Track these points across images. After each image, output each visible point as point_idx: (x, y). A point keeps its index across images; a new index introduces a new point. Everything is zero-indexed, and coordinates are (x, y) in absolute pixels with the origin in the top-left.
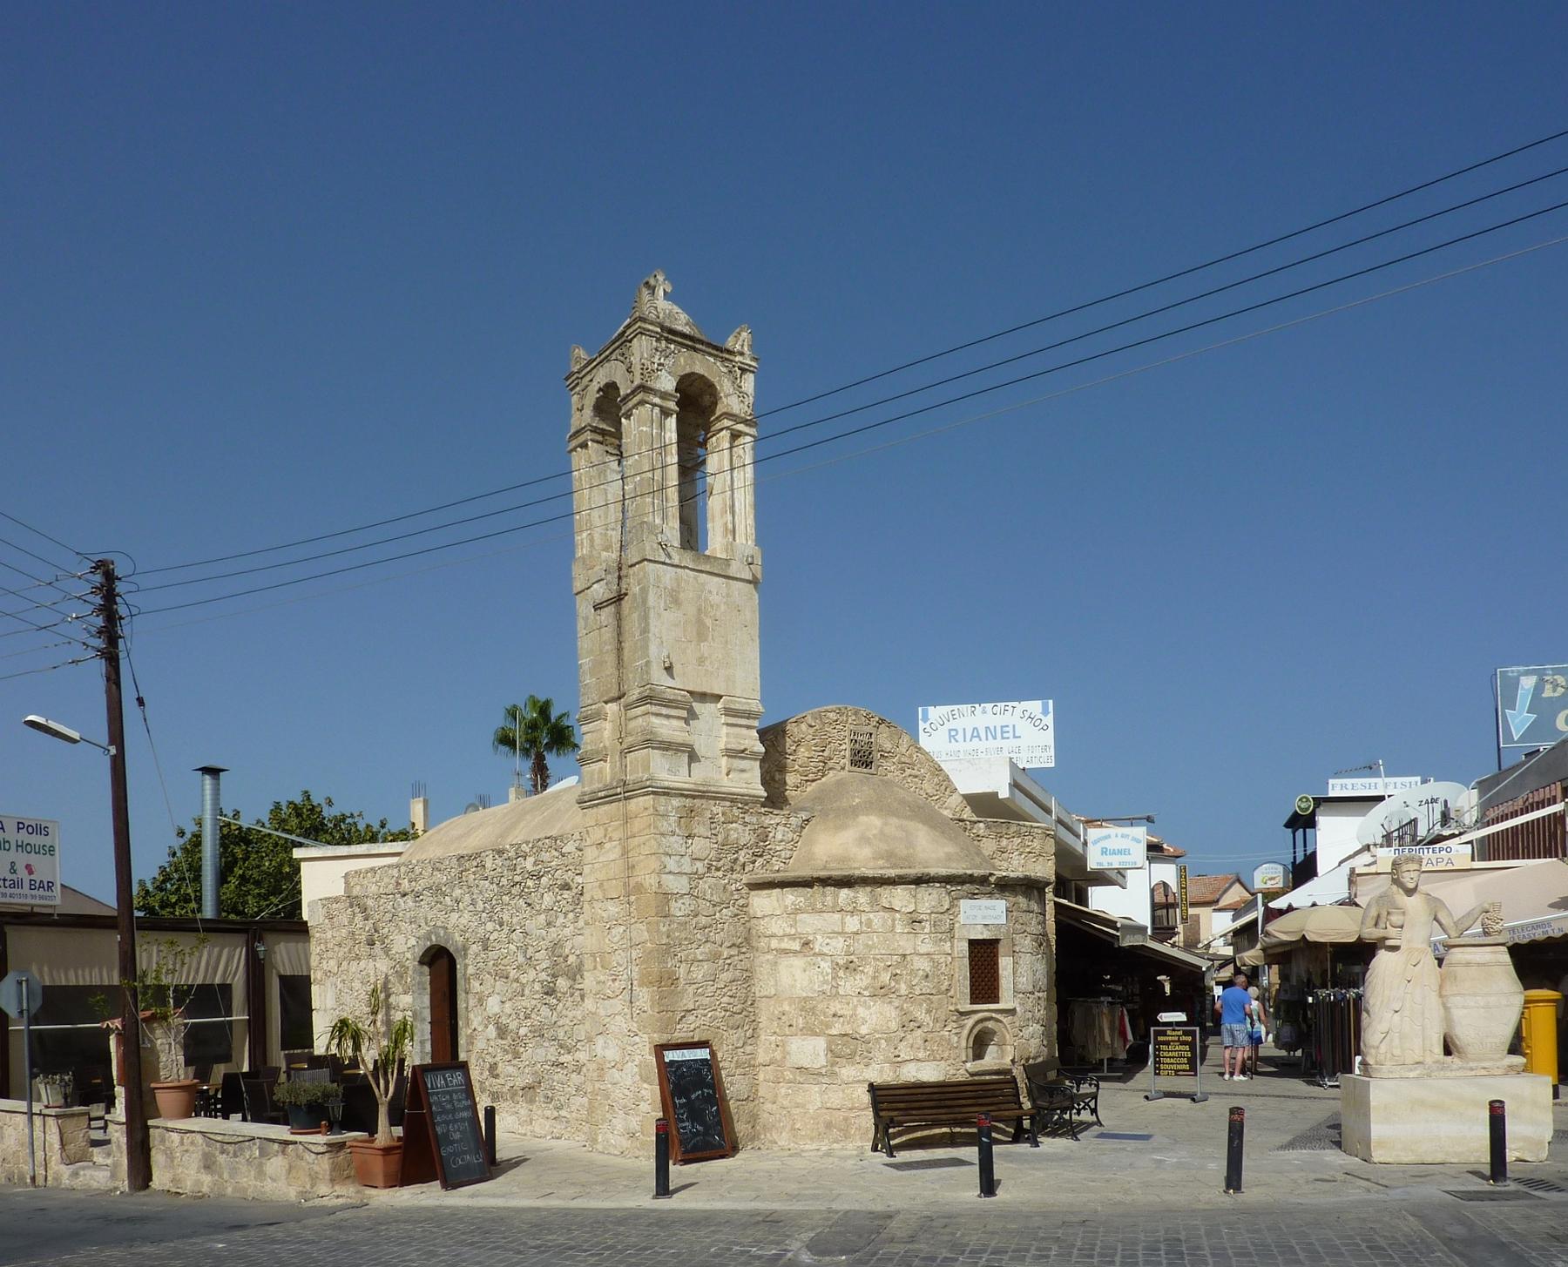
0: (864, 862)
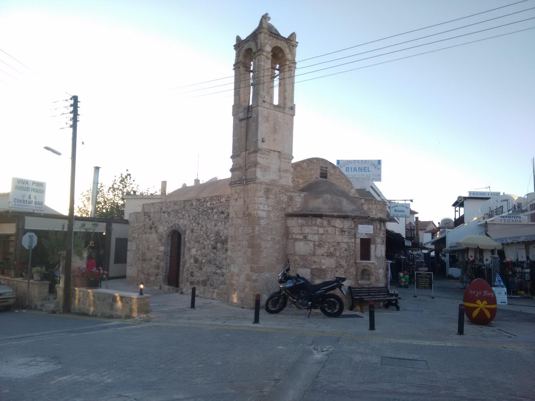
0: (325, 209)
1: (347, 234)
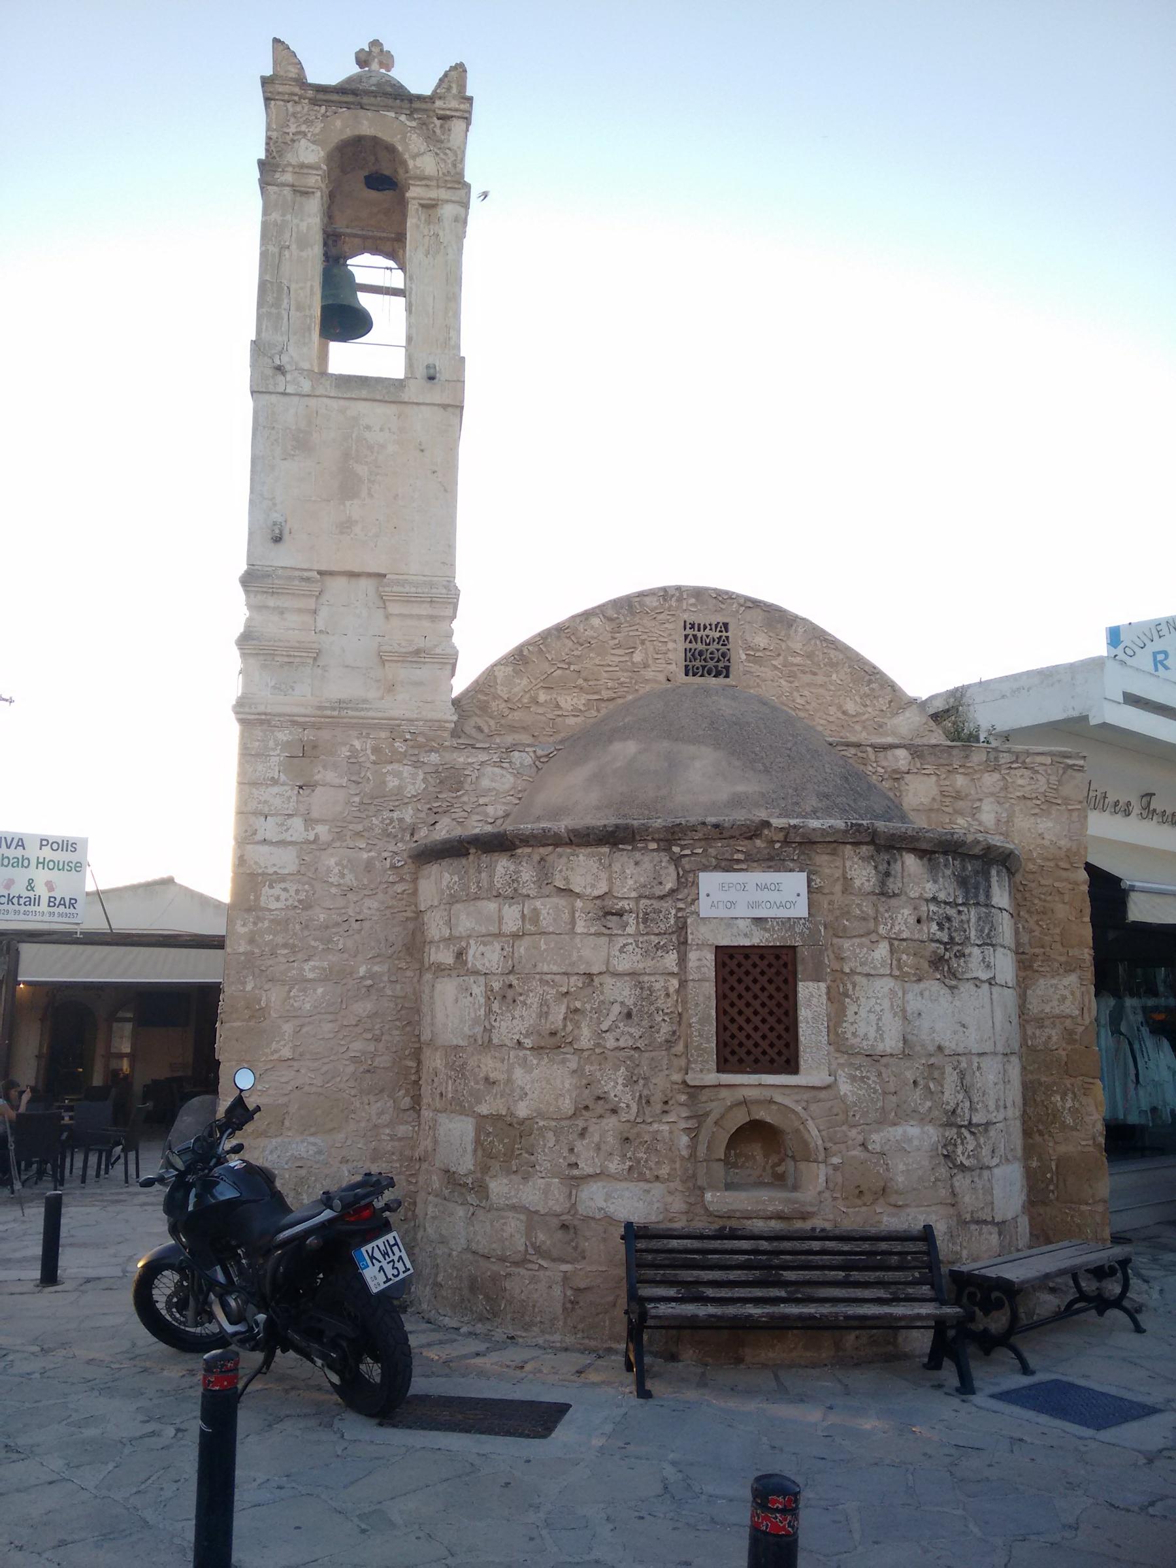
1: (631, 930)
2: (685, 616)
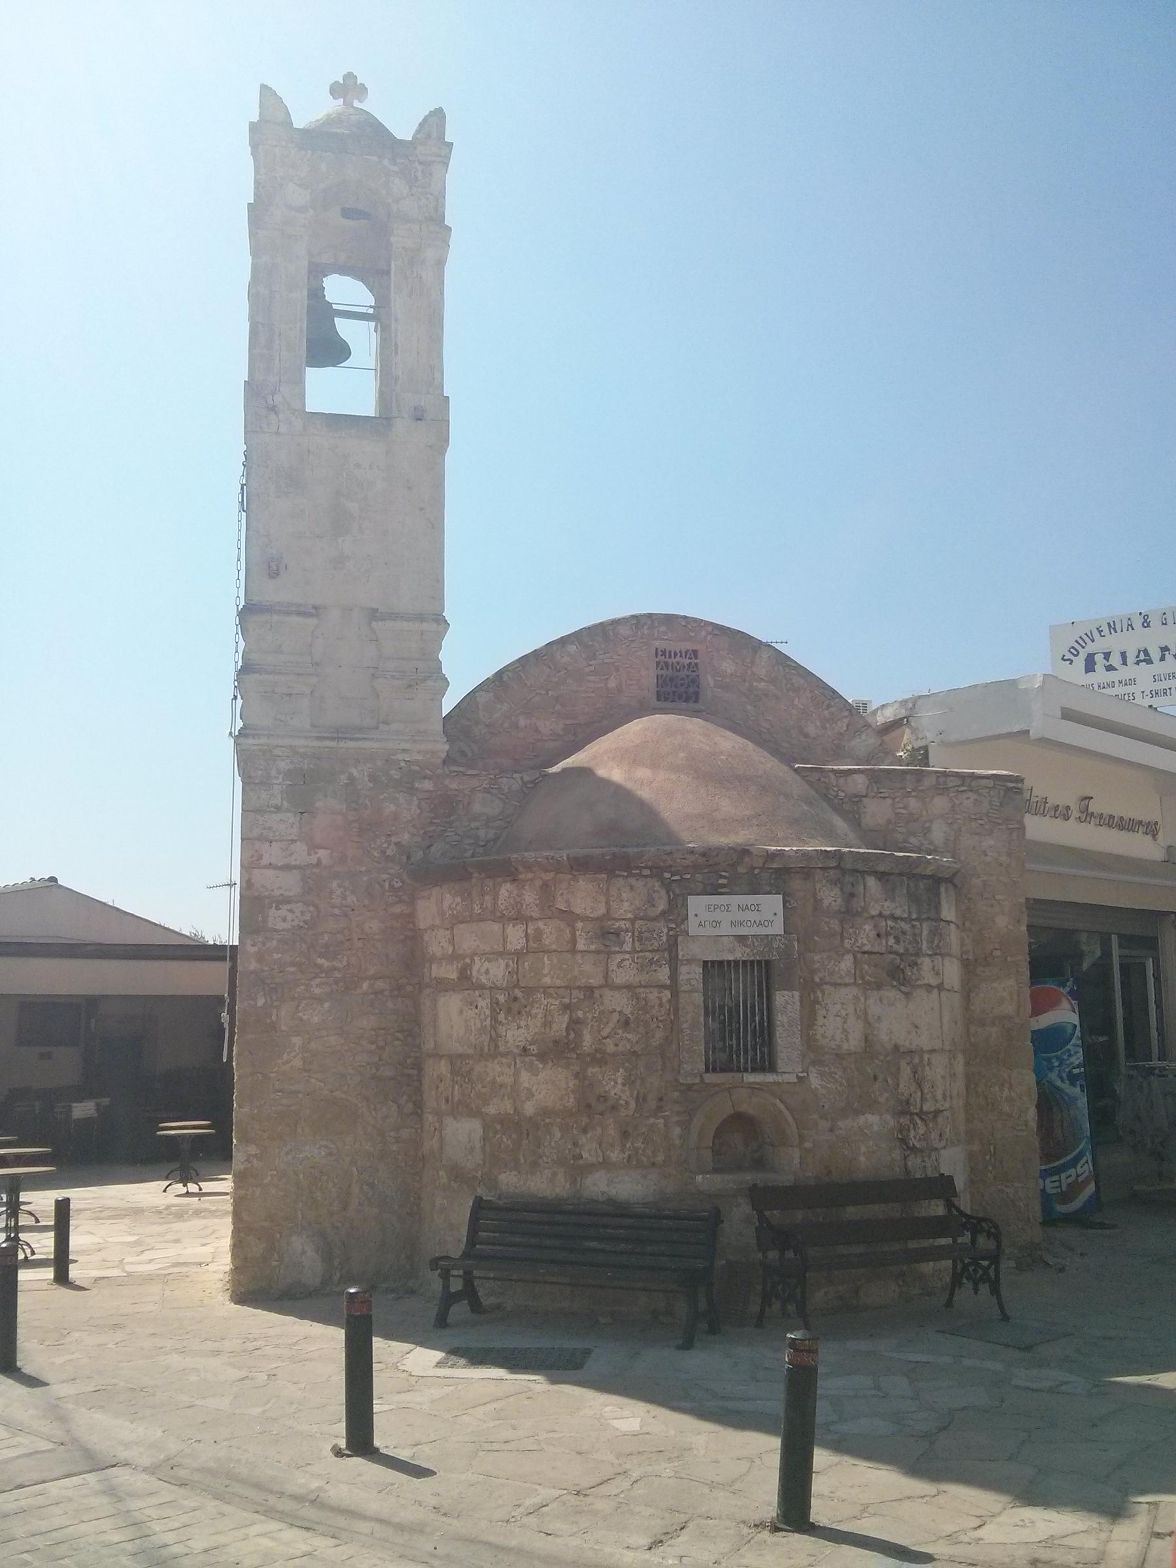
1: (627, 947)
2: (657, 643)
